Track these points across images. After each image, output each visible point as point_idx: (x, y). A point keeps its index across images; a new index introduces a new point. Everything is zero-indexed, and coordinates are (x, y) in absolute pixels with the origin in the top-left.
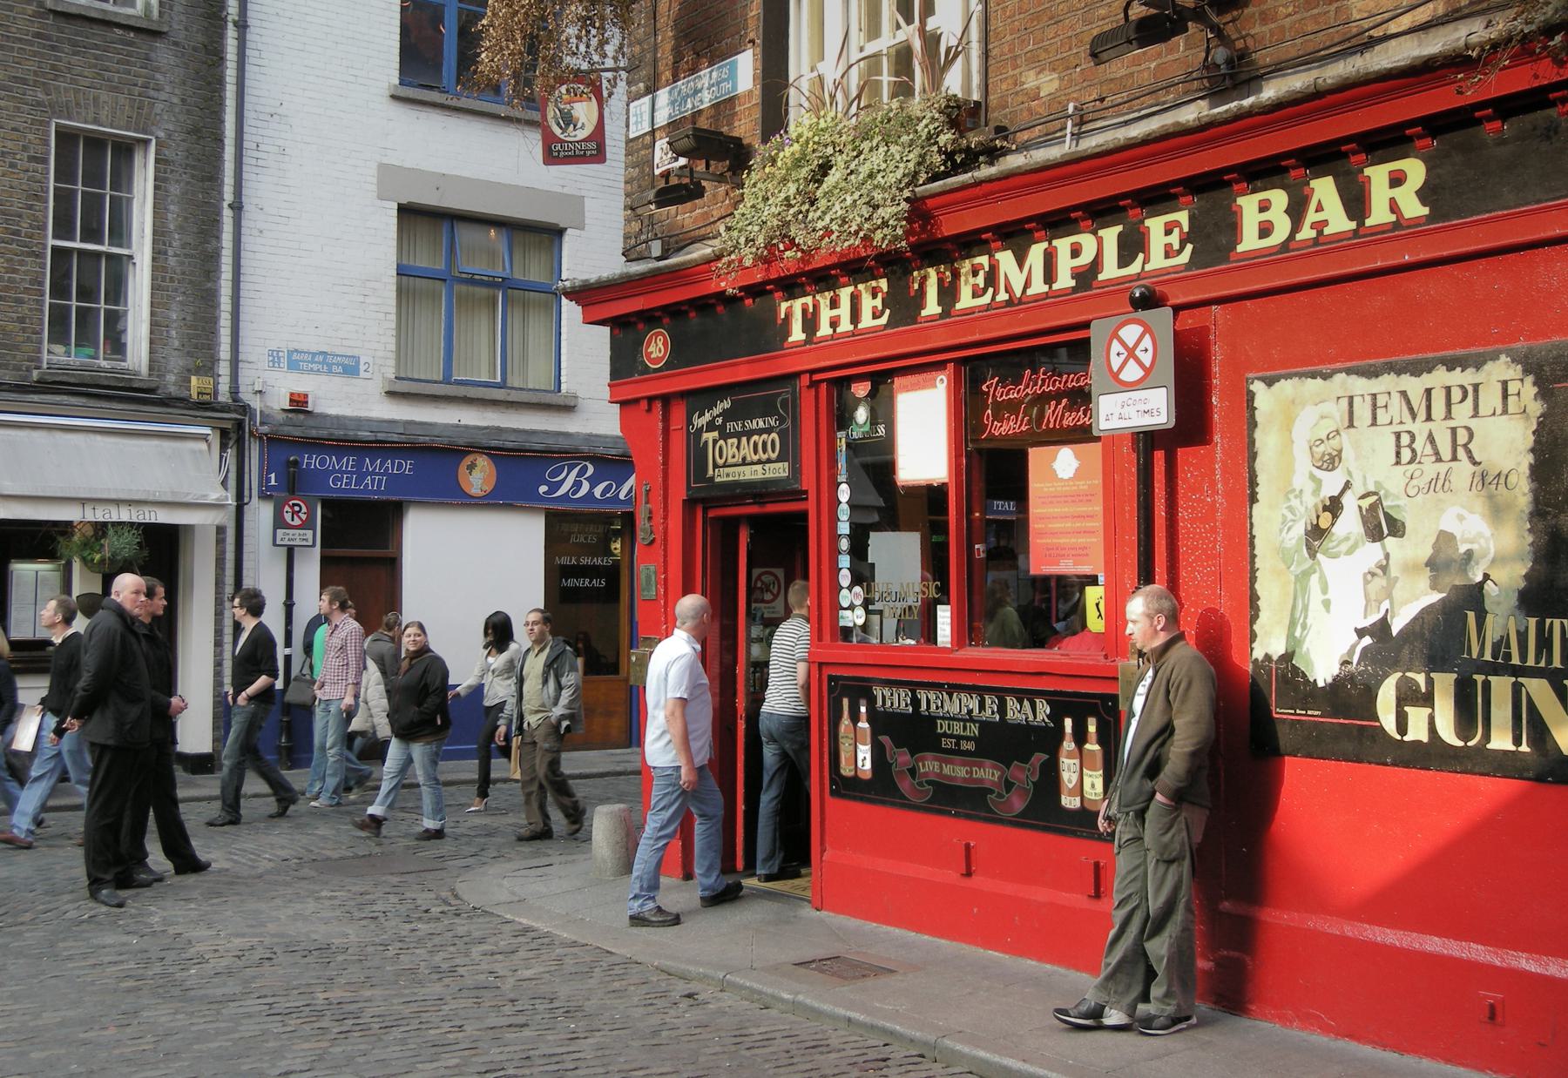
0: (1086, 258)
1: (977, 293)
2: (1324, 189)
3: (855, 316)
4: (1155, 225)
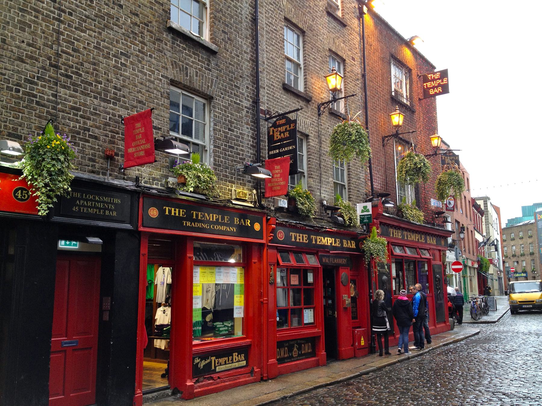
0: (331, 242)
1: (320, 242)
2: (349, 241)
3: (303, 240)
4: (337, 240)
